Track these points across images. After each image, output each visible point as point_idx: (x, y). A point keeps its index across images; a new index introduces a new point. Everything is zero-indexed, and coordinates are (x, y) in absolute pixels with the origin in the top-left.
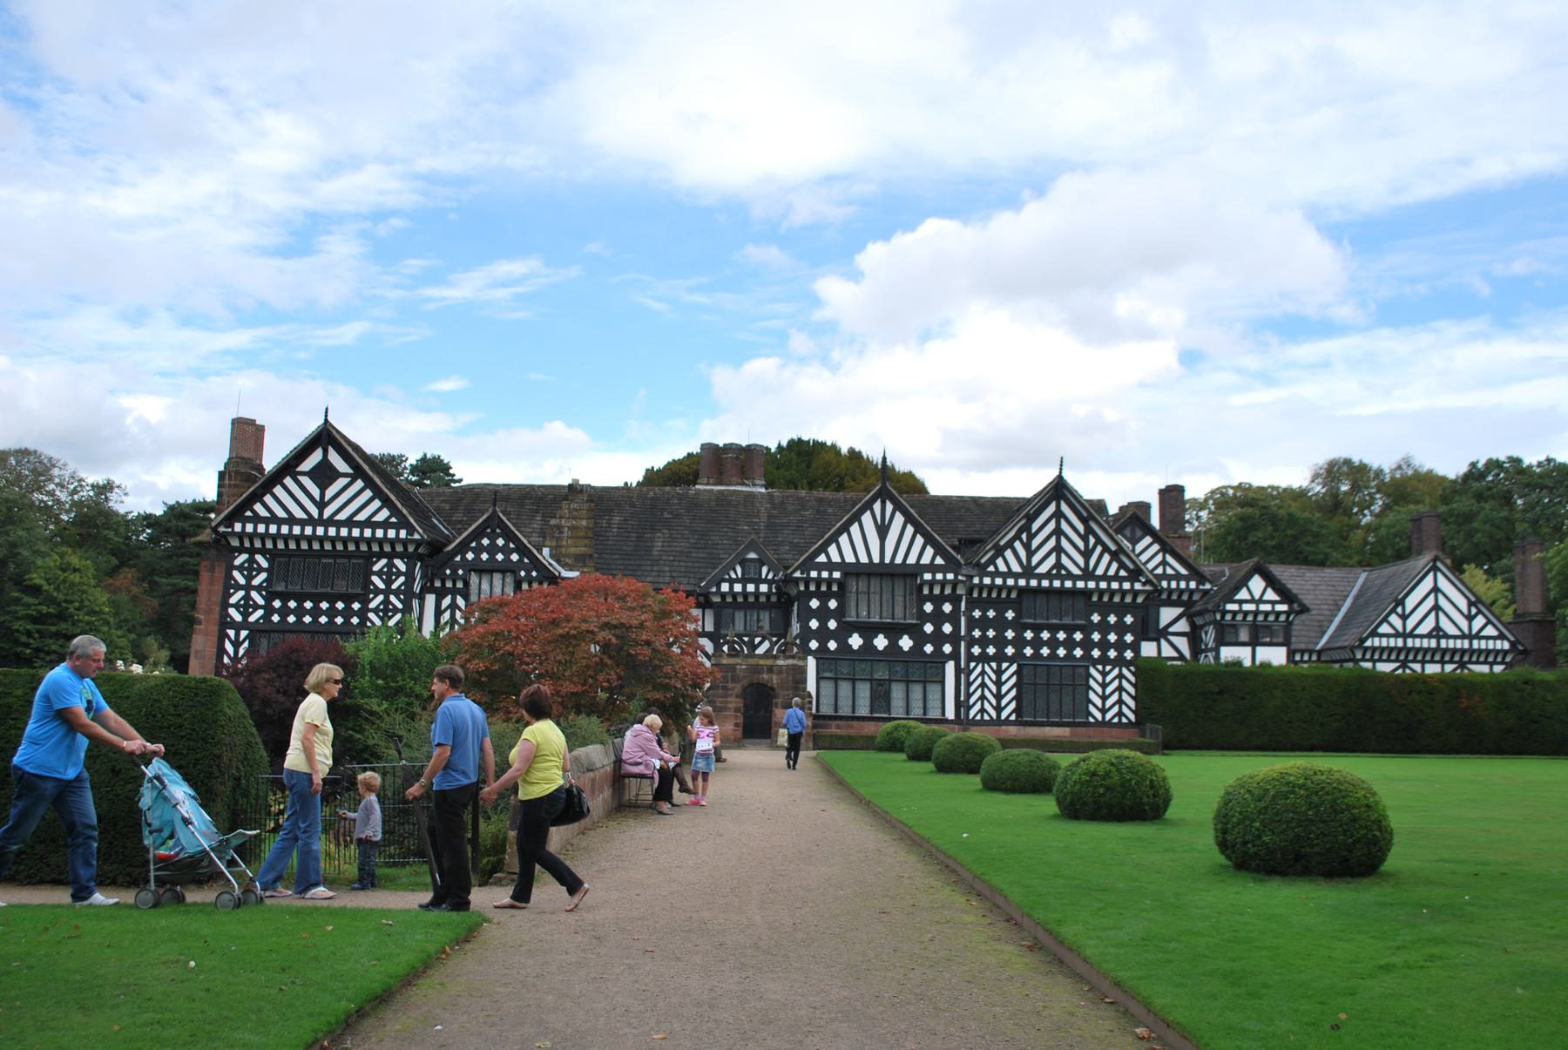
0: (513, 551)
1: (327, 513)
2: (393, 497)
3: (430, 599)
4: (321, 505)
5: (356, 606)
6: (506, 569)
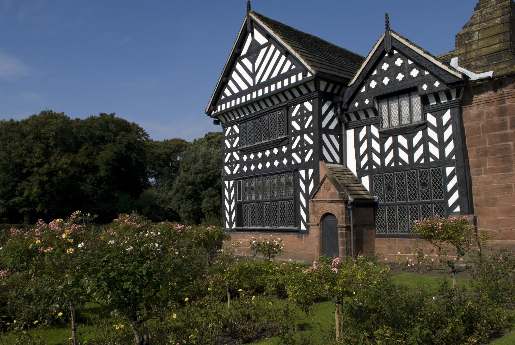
0: (411, 68)
1: (257, 79)
2: (289, 48)
3: (350, 134)
4: (253, 75)
5: (284, 149)
6: (407, 90)
